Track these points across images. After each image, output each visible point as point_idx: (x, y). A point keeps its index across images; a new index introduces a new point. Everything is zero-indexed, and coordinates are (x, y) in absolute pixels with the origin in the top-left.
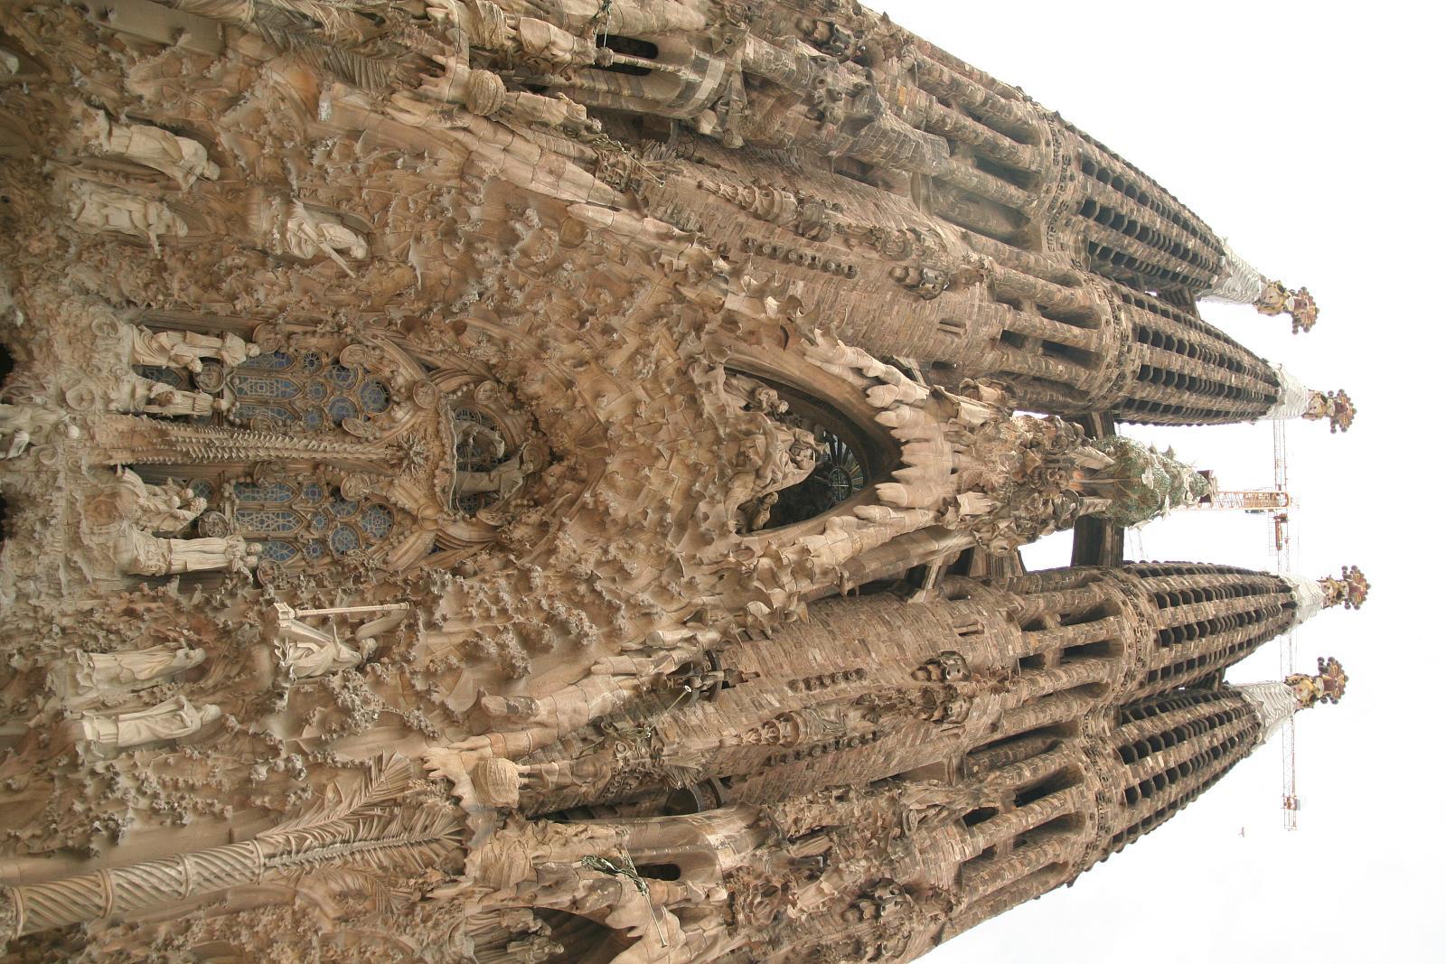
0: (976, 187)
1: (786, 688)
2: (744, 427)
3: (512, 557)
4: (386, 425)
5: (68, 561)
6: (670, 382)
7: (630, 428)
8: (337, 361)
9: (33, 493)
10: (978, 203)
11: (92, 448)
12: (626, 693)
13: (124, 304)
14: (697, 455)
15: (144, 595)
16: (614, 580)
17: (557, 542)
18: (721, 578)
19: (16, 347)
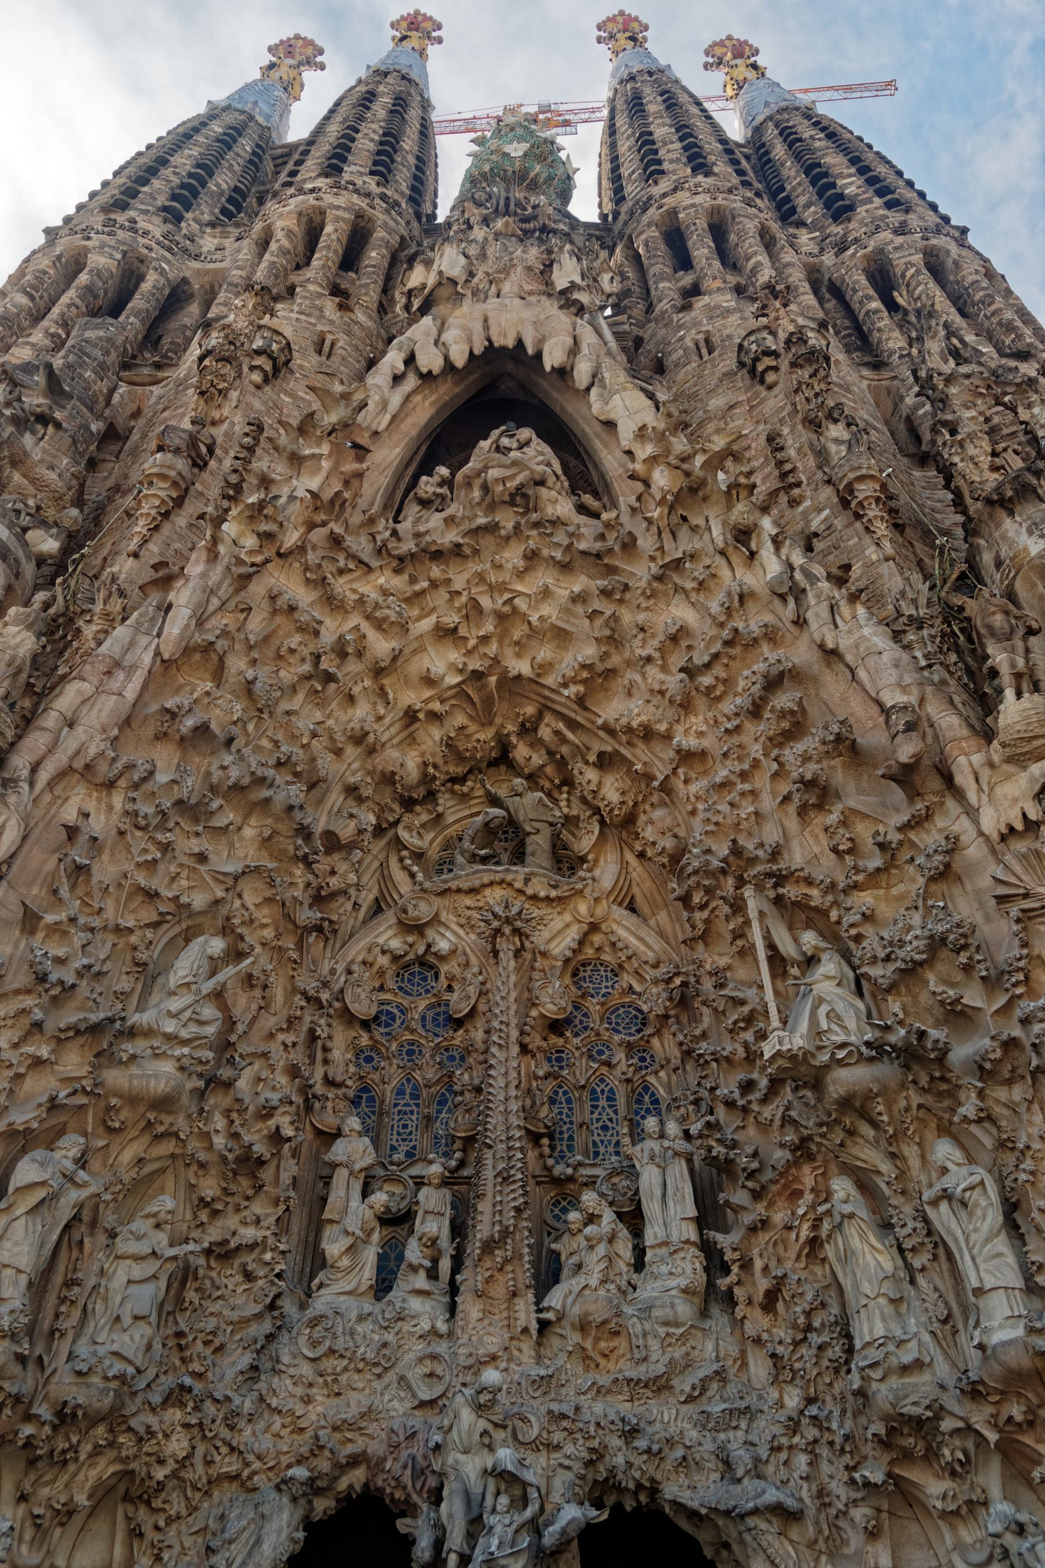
0: (142, 321)
1: (801, 509)
2: (477, 494)
3: (656, 784)
4: (462, 960)
5: (690, 1399)
6: (413, 580)
7: (472, 642)
8: (365, 1025)
9: (586, 1455)
10: (160, 337)
12: (861, 611)
13: (276, 1313)
14: (513, 556)
15: (738, 1283)
16: (689, 647)
17: (634, 724)
18: (684, 519)
19: (343, 1485)
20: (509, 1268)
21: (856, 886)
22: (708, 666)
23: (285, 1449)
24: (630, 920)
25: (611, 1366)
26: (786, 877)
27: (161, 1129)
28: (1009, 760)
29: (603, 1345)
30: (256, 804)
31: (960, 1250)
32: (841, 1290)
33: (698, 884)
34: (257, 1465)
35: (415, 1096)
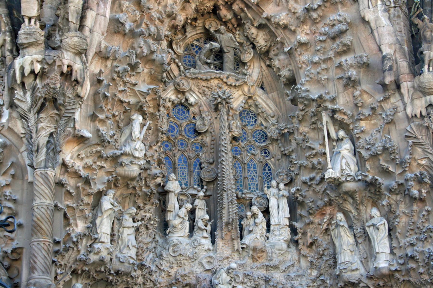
5: (284, 271)
11: (232, 258)
17: (281, 23)
20: (232, 231)
21: (361, 120)
22: (315, 10)
23: (165, 281)
24: (264, 96)
25: (260, 260)
26: (337, 111)
27: (131, 186)
28: (421, 91)
29: (259, 255)
30: (150, 60)
31: (374, 241)
32: (334, 244)
33: (303, 102)
34: (159, 285)
35: (185, 162)
